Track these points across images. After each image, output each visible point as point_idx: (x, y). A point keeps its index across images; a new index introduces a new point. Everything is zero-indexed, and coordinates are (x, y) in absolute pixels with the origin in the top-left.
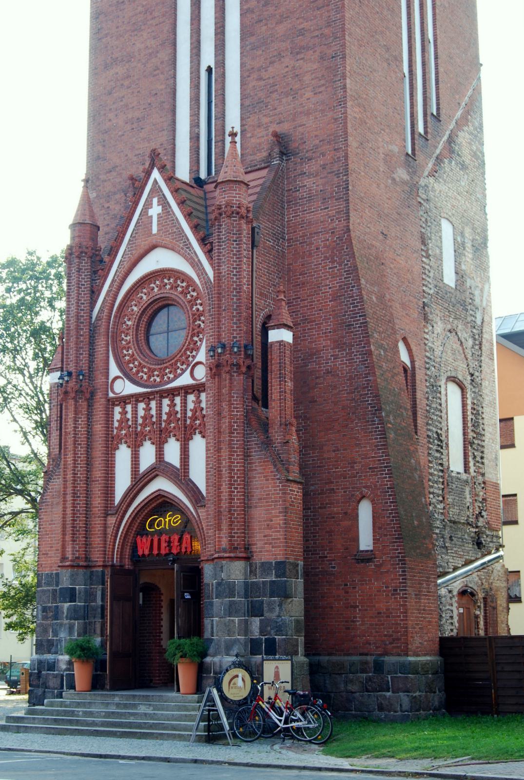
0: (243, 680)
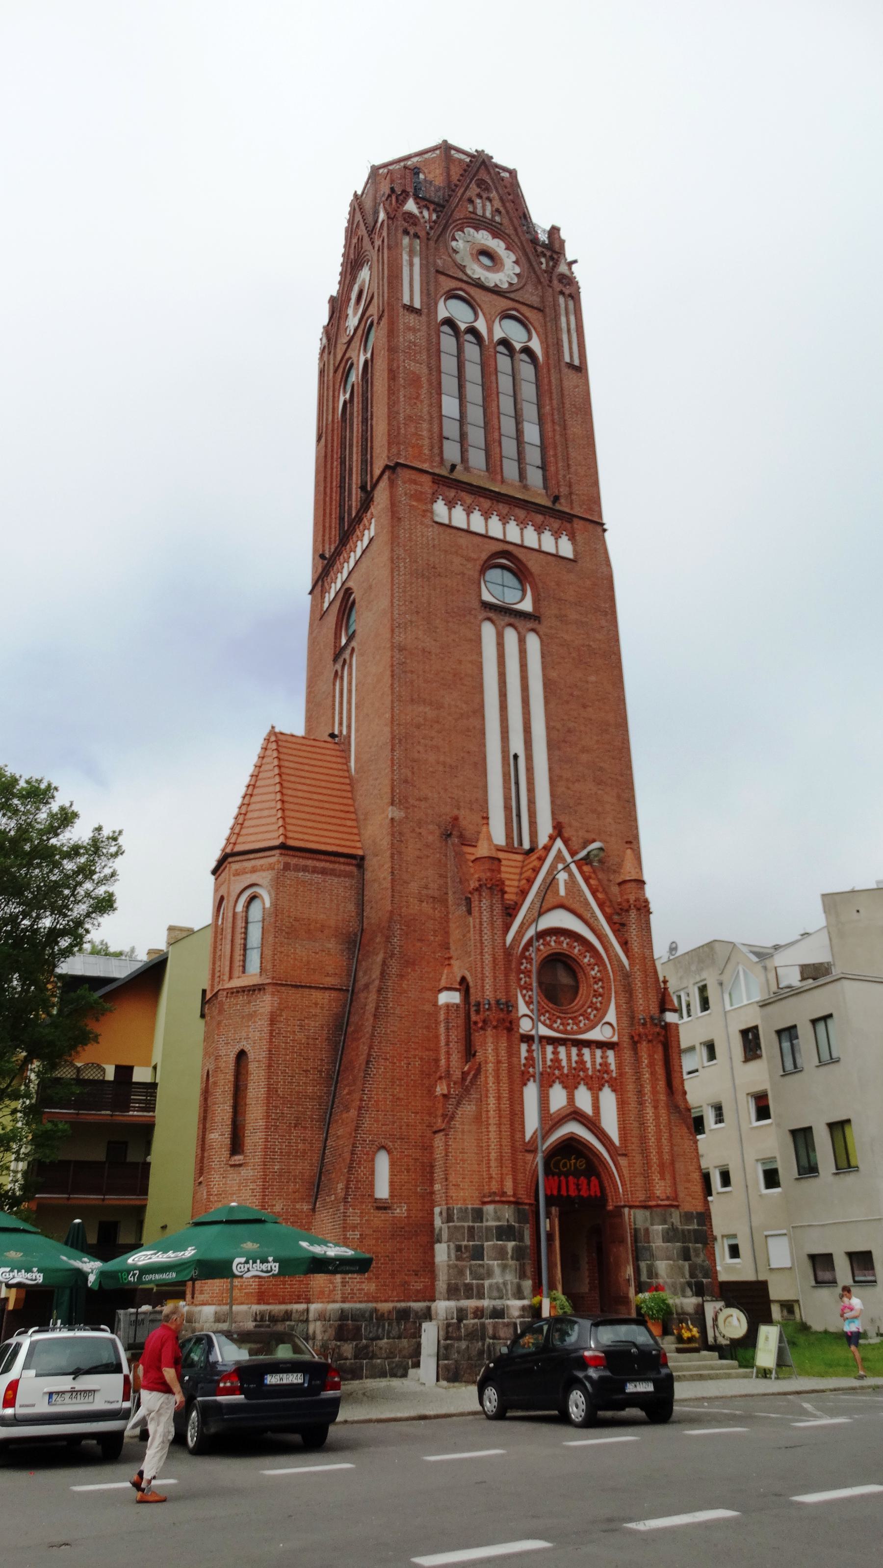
0: (738, 1320)
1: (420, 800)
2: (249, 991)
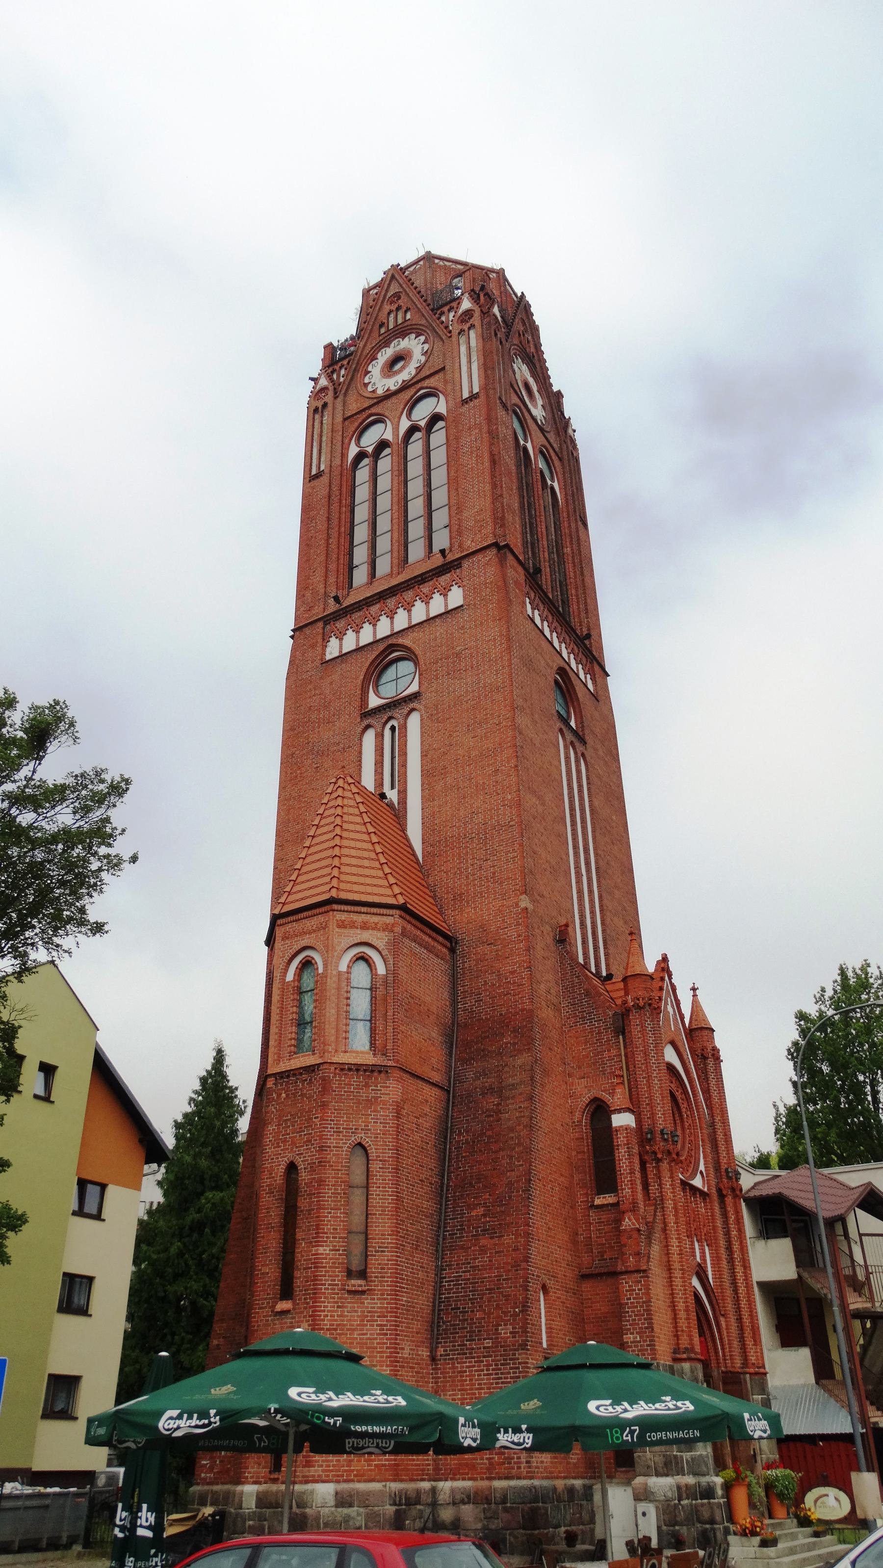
2: (365, 1071)
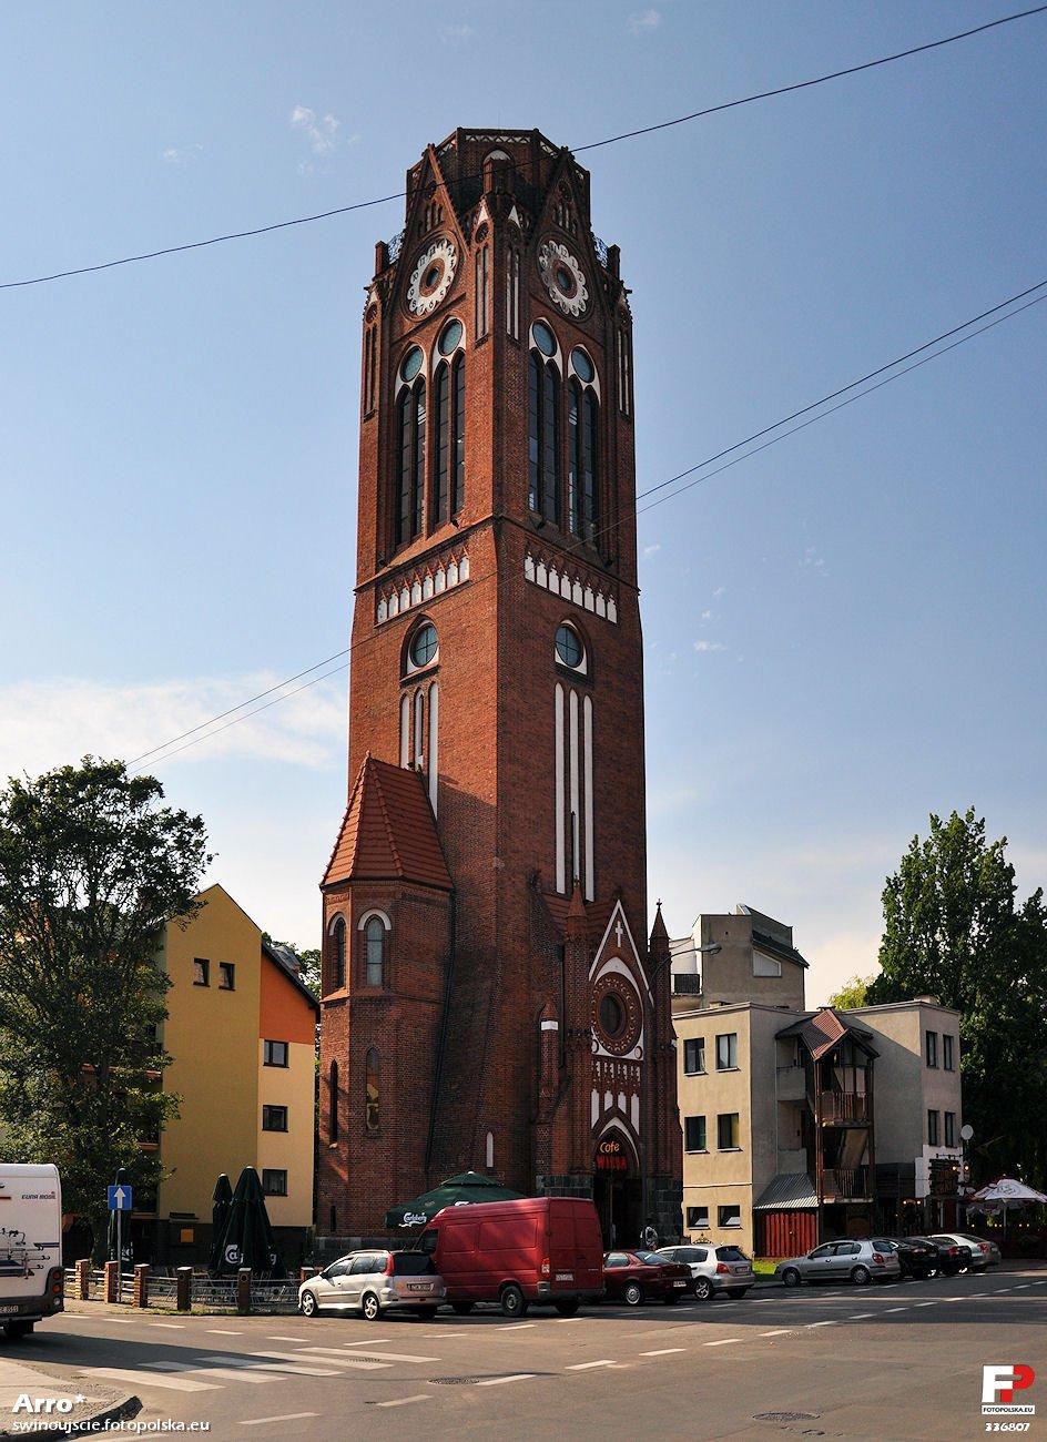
1: (513, 852)
